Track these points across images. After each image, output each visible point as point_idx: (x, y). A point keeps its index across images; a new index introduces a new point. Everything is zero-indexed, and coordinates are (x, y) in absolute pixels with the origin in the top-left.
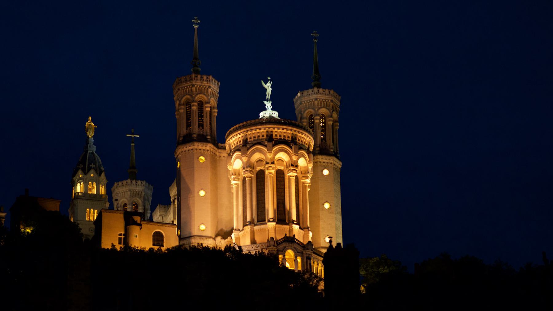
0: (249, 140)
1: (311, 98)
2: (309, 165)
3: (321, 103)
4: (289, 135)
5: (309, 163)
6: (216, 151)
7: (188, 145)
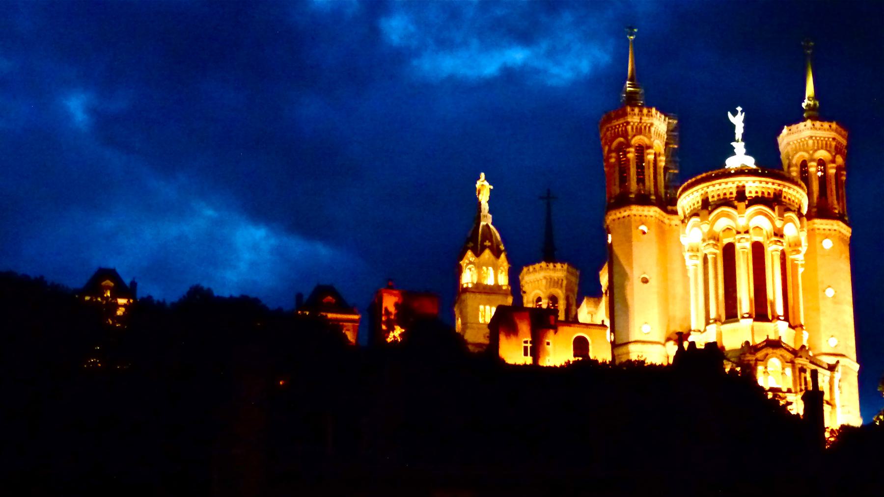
0: (710, 200)
1: (803, 136)
2: (801, 233)
3: (818, 143)
4: (770, 191)
5: (801, 231)
6: (664, 217)
7: (622, 210)
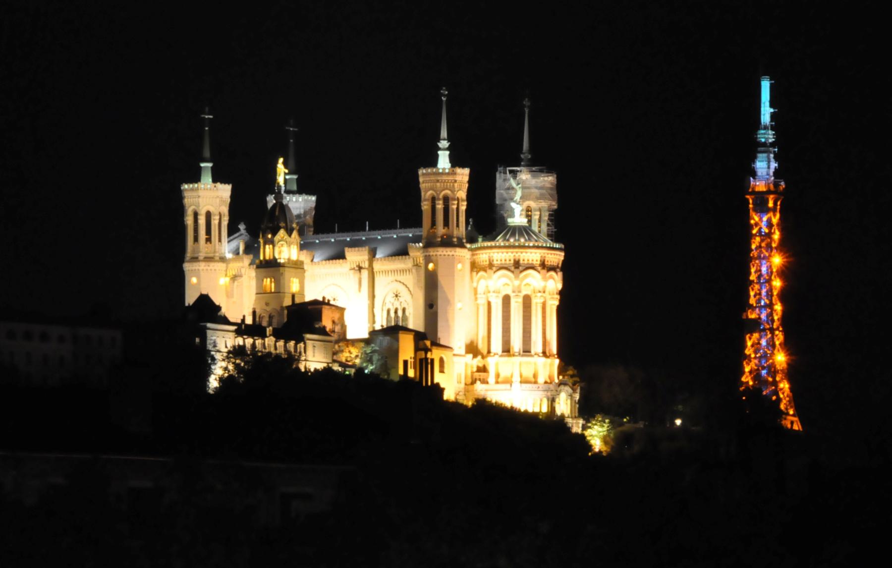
0: (521, 262)
